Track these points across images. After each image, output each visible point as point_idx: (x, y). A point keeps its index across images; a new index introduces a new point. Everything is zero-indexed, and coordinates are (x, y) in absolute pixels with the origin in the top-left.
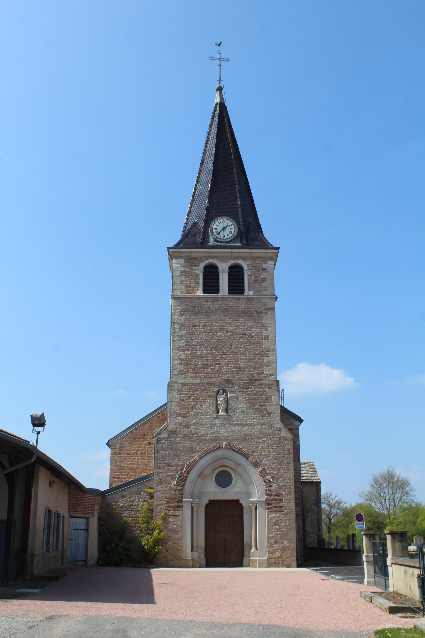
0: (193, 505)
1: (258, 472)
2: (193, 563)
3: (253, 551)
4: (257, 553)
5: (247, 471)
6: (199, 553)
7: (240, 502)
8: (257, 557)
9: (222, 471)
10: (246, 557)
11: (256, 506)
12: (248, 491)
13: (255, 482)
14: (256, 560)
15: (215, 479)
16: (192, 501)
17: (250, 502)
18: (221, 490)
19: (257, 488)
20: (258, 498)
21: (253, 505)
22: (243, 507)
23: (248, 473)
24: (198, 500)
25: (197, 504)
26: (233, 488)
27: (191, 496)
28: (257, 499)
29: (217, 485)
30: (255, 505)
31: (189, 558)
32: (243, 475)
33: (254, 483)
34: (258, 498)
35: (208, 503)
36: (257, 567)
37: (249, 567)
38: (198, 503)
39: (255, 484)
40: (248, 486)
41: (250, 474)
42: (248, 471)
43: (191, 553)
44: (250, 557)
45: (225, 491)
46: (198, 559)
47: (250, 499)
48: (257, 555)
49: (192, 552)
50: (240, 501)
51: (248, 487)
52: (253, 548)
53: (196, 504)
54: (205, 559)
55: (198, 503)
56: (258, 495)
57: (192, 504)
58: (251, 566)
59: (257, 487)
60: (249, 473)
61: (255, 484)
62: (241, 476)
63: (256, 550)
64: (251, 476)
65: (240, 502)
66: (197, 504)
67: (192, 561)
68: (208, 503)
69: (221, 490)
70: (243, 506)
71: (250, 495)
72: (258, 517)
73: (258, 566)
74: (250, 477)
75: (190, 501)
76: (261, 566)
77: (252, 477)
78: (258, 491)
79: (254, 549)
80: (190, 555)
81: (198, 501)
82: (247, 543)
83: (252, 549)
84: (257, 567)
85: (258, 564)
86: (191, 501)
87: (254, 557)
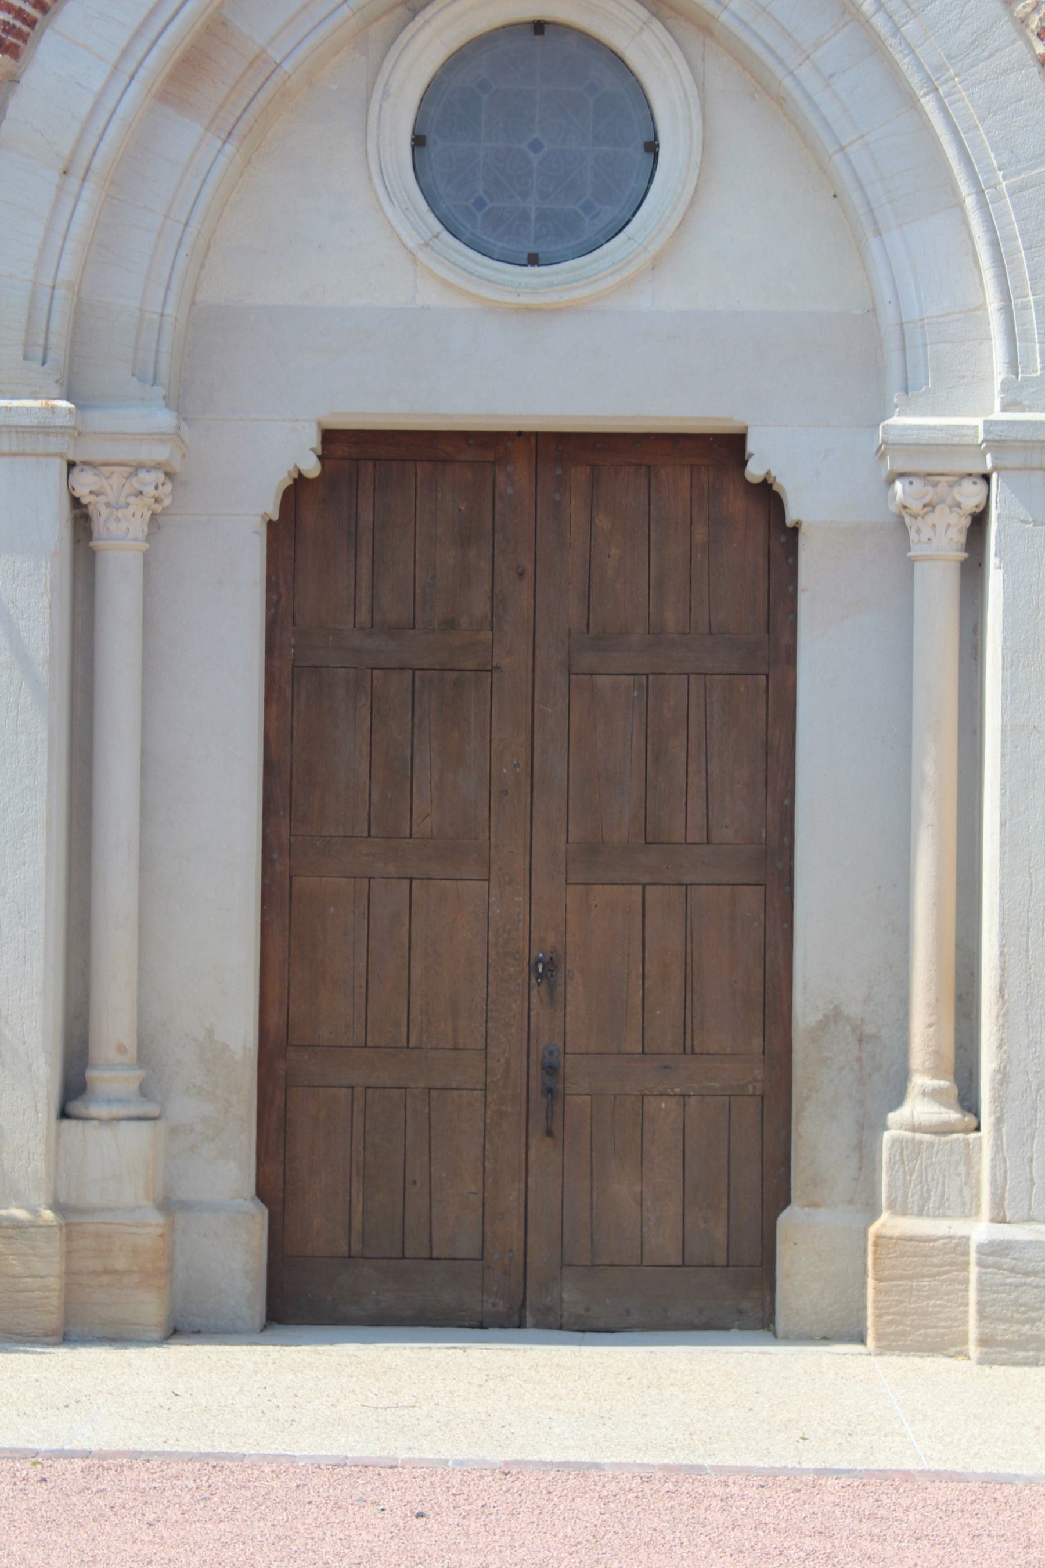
0: (85, 483)
1: (1024, 21)
2: (70, 1274)
3: (914, 1129)
4: (969, 1156)
5: (864, 23)
6: (174, 1131)
7: (754, 471)
8: (969, 1211)
9: (511, 29)
10: (815, 1205)
11: (979, 521)
12: (874, 310)
13: (973, 177)
14: (961, 1245)
15: (418, 141)
16: (78, 434)
17: (889, 465)
18: (487, 293)
19: (999, 262)
20: (1004, 409)
21: (930, 506)
22: (795, 530)
23: (876, 47)
24: (164, 419)
25: (150, 479)
26: (656, 264)
27: (58, 353)
28: (998, 415)
29: (438, 227)
30: (970, 496)
31: (20, 1214)
32: (803, 72)
33: (964, 188)
34: (1004, 409)
35: (311, 467)
36: (965, 1355)
37: (861, 1340)
38: (157, 466)
39: (970, 202)
40: (878, 233)
41: (905, 64)
42: (878, 21)
43: (56, 1148)
44: (873, 1211)
45: (554, 311)
46: (156, 1218)
47: (896, 420)
48: (972, 1181)
49: (66, 1123)
50: (751, 446)
51: (873, 243)
52: (920, 1081)
53: (138, 467)
54: (258, 1218)
55: (161, 453)
56: (1013, 365)
57: (71, 465)
58: (879, 1337)
59: (994, 244)
60: (892, 42)
61: (970, 202)
62: (780, 100)
63: (954, 1115)
64: (915, 80)
65: (754, 471)
66: (150, 479)
67: (69, 1254)
68: (311, 467)
69: (487, 293)
70: (792, 515)
71: (894, 359)
72: (1008, 664)
73: (984, 1341)
74: (912, 102)
75: (44, 430)
76: (1022, 1343)
77: (928, 103)
78: (1007, 309)
79: (935, 1095)
80: (39, 1166)
81: (158, 437)
82: (835, 1016)
83: (898, 1099)
84: (973, 1349)
85: (982, 1315)
86: (61, 431)
87: (920, 1213)
